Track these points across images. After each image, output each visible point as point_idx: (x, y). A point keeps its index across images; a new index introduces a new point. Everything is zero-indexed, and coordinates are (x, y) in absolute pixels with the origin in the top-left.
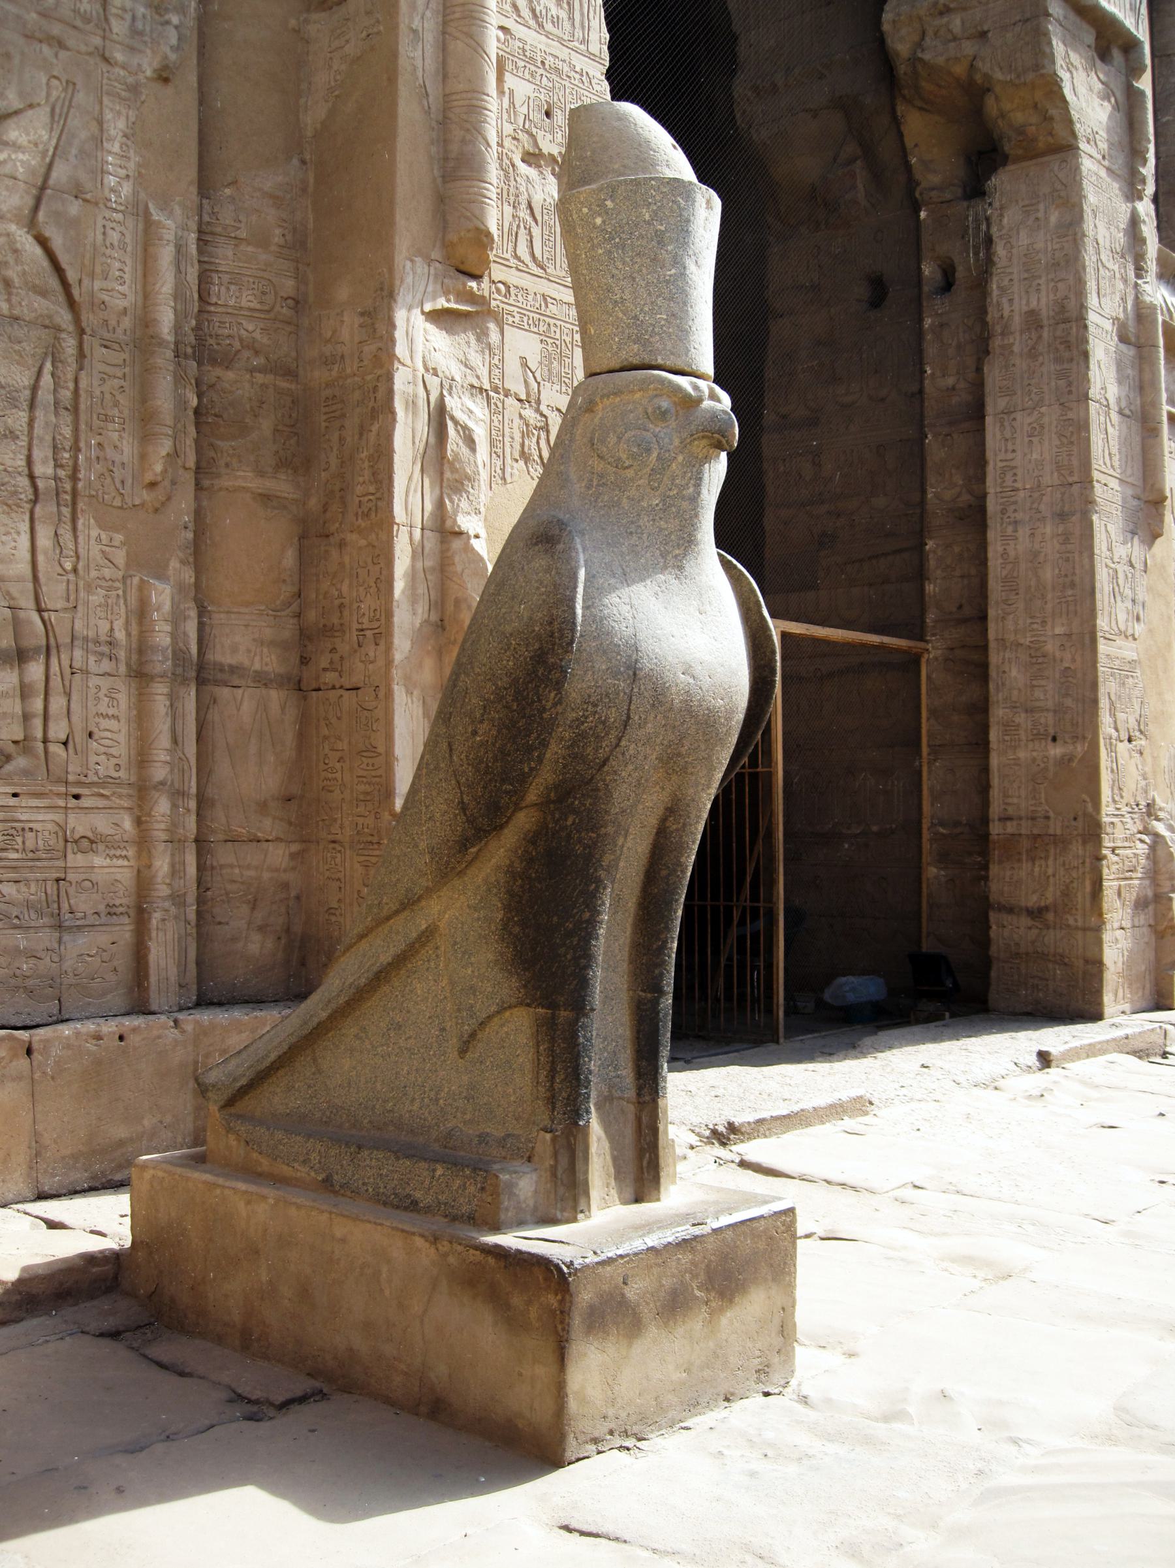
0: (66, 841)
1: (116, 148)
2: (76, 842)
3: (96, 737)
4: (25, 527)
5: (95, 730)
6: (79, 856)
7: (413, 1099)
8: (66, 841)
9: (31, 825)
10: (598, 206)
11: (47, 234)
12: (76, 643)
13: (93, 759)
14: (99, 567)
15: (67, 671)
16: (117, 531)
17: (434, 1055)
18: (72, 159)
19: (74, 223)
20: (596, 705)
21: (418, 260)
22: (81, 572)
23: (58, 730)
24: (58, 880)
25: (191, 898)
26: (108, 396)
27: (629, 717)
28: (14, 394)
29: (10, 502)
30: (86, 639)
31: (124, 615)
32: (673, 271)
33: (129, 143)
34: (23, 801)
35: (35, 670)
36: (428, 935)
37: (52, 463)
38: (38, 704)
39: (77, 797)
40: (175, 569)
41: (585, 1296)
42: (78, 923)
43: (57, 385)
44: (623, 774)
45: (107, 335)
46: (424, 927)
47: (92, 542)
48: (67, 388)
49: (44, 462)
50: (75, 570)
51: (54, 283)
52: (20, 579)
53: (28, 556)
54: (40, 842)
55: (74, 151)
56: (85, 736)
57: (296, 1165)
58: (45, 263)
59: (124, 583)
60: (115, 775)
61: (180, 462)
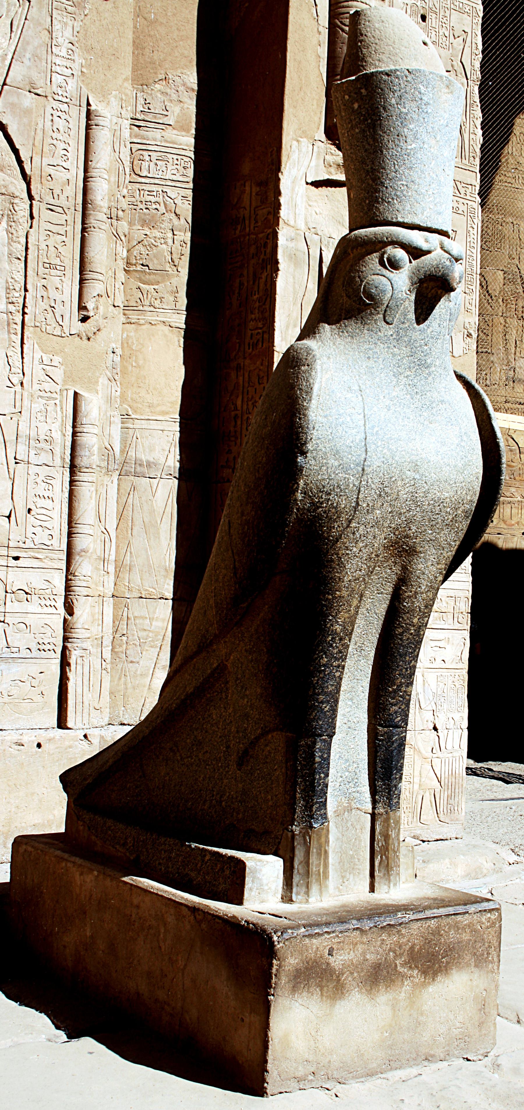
0: (6, 592)
1: (64, 53)
3: (32, 513)
5: (33, 507)
6: (16, 603)
7: (206, 801)
8: (6, 592)
10: (356, 93)
13: (30, 530)
15: (12, 461)
17: (221, 766)
18: (27, 62)
20: (330, 494)
21: (304, 141)
25: (107, 641)
26: (52, 249)
27: (357, 504)
31: (60, 420)
32: (414, 146)
33: (74, 48)
36: (221, 670)
37: (5, 300)
39: (16, 558)
40: (103, 385)
41: (289, 961)
42: (13, 655)
44: (355, 549)
45: (52, 201)
46: (215, 665)
47: (36, 362)
50: (22, 384)
56: (25, 511)
57: (118, 847)
59: (61, 395)
61: (110, 301)
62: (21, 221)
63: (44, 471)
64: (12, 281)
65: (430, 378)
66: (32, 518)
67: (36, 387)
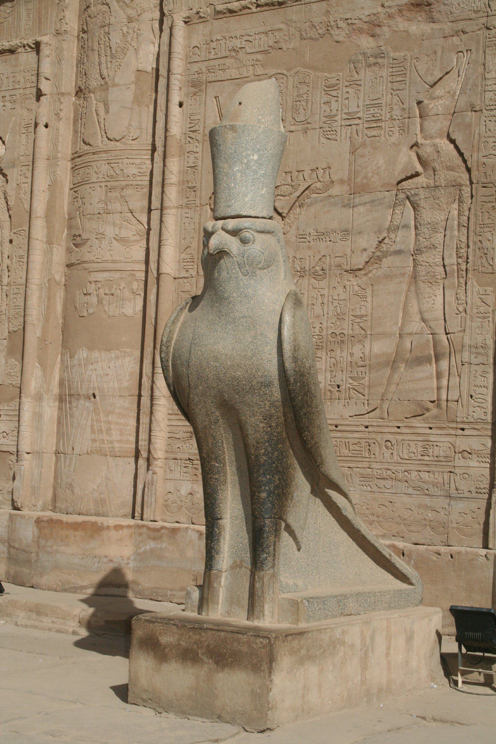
0: (455, 453)
3: (473, 398)
5: (473, 394)
8: (455, 453)
9: (437, 444)
11: (453, 138)
12: (464, 349)
13: (471, 409)
14: (478, 307)
15: (460, 363)
16: (489, 286)
18: (468, 92)
19: (469, 126)
22: (468, 311)
23: (454, 395)
24: (450, 472)
28: (436, 226)
29: (431, 281)
30: (470, 346)
34: (433, 431)
38: (444, 382)
39: (463, 429)
42: (459, 496)
43: (459, 215)
47: (475, 294)
48: (465, 215)
50: (465, 311)
54: (441, 452)
55: (469, 87)
60: (484, 418)
62: (465, 200)
63: (480, 369)
64: (460, 242)
65: (231, 305)
66: (473, 401)
67: (475, 311)
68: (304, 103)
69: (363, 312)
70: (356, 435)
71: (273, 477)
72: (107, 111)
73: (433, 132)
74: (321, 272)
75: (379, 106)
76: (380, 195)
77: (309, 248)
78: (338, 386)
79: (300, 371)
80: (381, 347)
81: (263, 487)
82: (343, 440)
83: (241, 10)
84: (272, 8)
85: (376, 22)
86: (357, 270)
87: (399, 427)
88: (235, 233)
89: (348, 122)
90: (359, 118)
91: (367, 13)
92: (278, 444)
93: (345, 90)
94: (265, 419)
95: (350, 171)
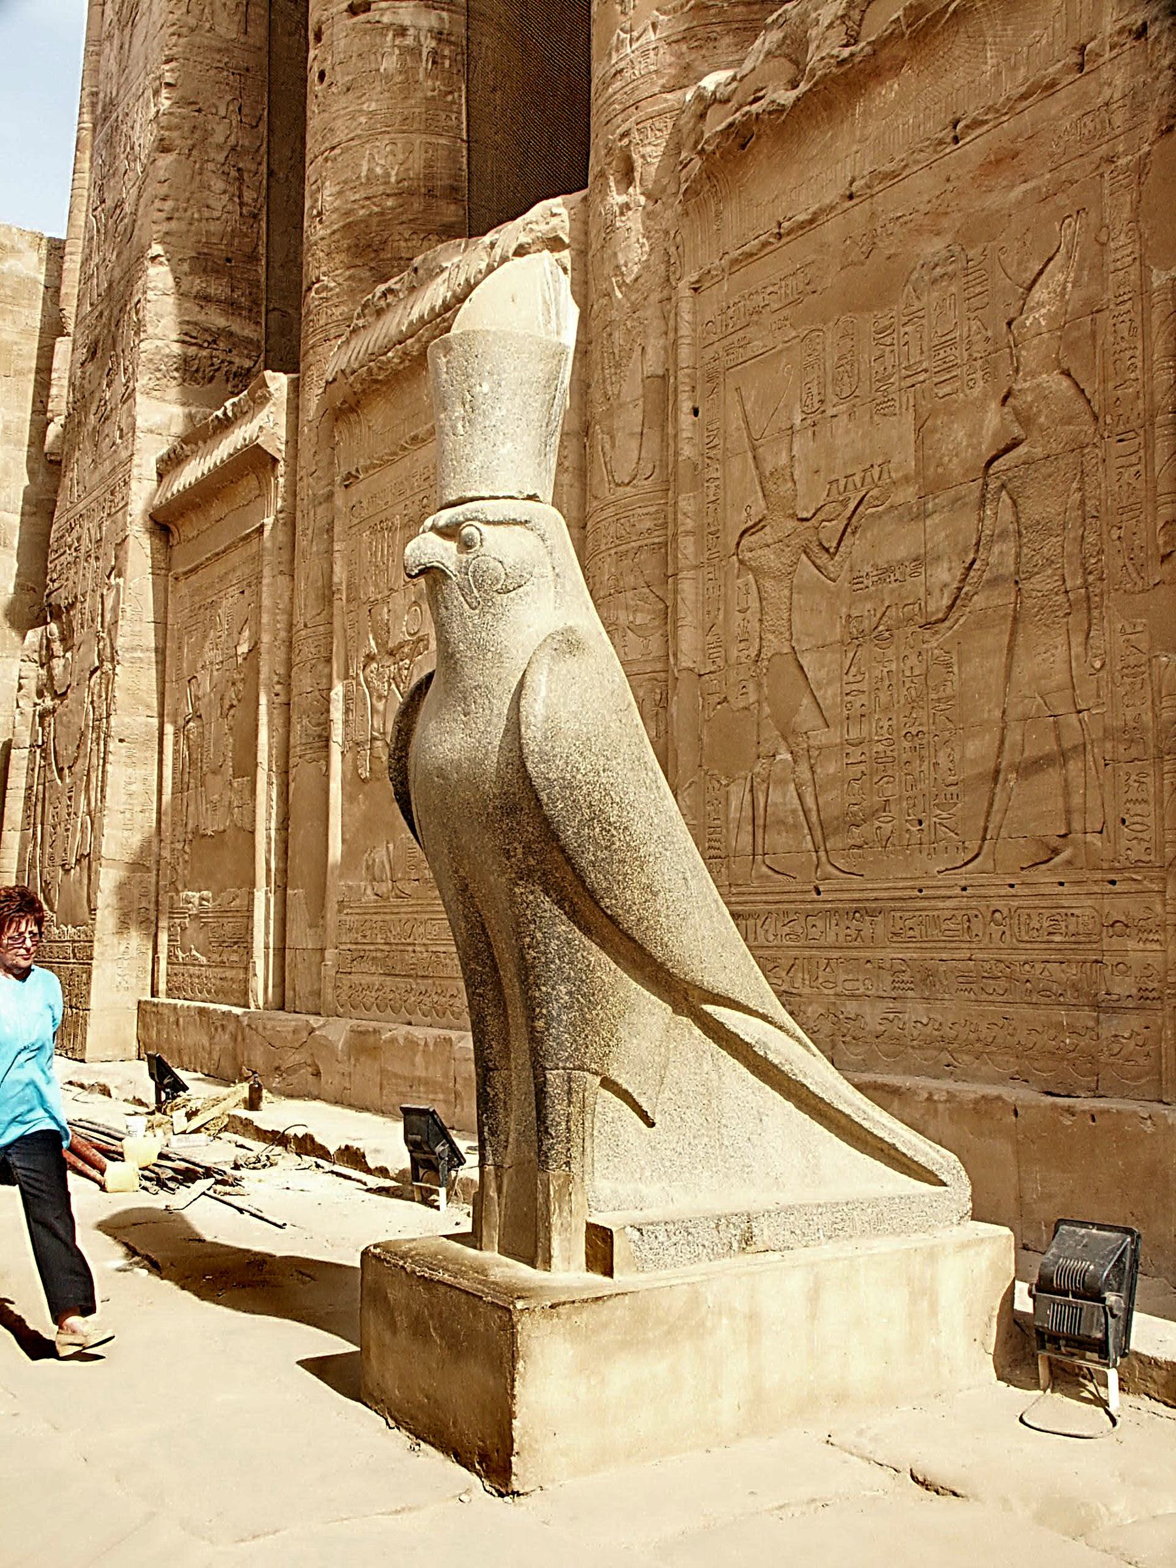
2: (1112, 926)
4: (1061, 640)
9: (1073, 911)
13: (1124, 843)
16: (1140, 616)
24: (1097, 961)
35: (1074, 766)
39: (1113, 882)
49: (1074, 575)
51: (1080, 405)
52: (1060, 689)
53: (1066, 666)
54: (1080, 926)
56: (1119, 821)
58: (1072, 391)
60: (1147, 858)
68: (848, 367)
69: (949, 691)
70: (949, 903)
71: (553, 989)
72: (613, 446)
73: (1034, 365)
74: (887, 634)
75: (952, 343)
76: (963, 490)
77: (869, 597)
78: (920, 823)
79: (563, 778)
80: (979, 748)
81: (538, 1010)
82: (930, 913)
83: (760, 250)
84: (800, 232)
85: (941, 210)
86: (936, 622)
87: (1012, 886)
88: (449, 532)
89: (909, 381)
90: (926, 371)
91: (926, 198)
92: (555, 924)
93: (903, 330)
94: (521, 879)
95: (917, 460)
